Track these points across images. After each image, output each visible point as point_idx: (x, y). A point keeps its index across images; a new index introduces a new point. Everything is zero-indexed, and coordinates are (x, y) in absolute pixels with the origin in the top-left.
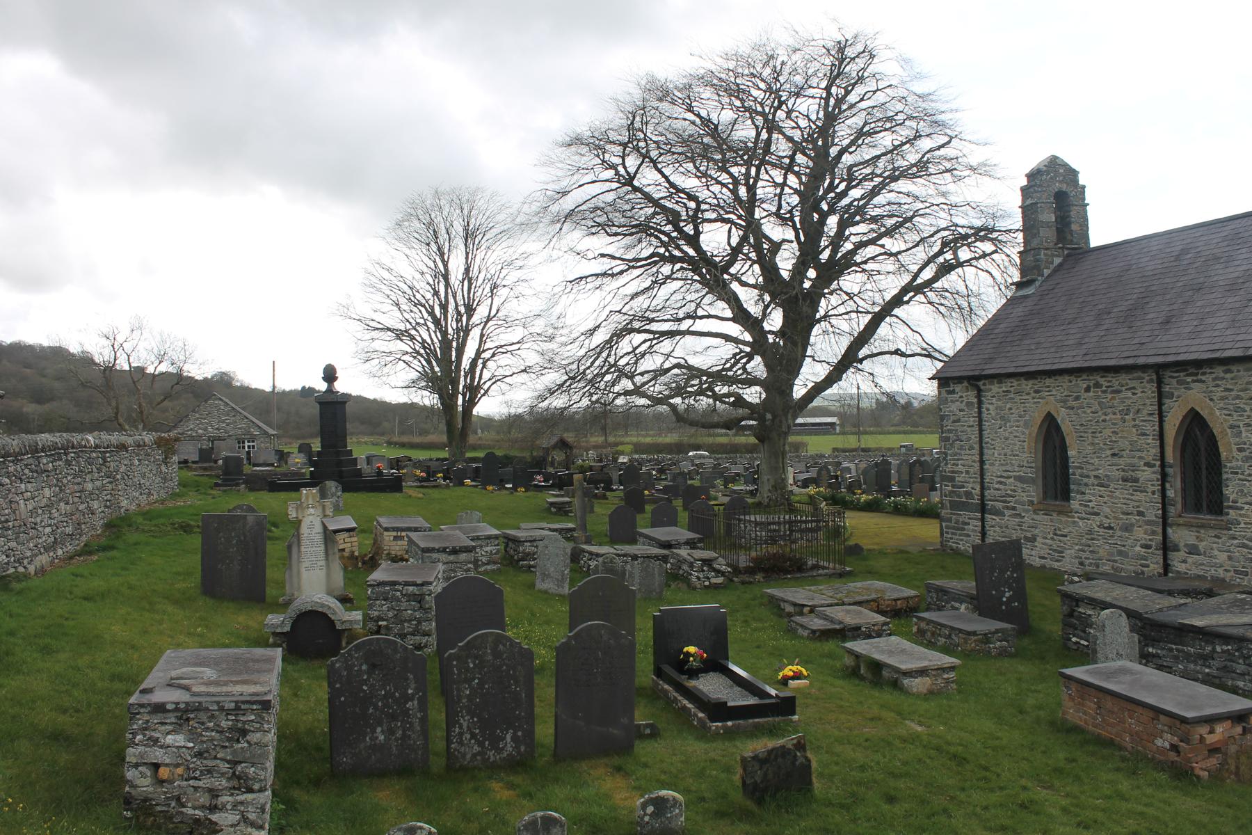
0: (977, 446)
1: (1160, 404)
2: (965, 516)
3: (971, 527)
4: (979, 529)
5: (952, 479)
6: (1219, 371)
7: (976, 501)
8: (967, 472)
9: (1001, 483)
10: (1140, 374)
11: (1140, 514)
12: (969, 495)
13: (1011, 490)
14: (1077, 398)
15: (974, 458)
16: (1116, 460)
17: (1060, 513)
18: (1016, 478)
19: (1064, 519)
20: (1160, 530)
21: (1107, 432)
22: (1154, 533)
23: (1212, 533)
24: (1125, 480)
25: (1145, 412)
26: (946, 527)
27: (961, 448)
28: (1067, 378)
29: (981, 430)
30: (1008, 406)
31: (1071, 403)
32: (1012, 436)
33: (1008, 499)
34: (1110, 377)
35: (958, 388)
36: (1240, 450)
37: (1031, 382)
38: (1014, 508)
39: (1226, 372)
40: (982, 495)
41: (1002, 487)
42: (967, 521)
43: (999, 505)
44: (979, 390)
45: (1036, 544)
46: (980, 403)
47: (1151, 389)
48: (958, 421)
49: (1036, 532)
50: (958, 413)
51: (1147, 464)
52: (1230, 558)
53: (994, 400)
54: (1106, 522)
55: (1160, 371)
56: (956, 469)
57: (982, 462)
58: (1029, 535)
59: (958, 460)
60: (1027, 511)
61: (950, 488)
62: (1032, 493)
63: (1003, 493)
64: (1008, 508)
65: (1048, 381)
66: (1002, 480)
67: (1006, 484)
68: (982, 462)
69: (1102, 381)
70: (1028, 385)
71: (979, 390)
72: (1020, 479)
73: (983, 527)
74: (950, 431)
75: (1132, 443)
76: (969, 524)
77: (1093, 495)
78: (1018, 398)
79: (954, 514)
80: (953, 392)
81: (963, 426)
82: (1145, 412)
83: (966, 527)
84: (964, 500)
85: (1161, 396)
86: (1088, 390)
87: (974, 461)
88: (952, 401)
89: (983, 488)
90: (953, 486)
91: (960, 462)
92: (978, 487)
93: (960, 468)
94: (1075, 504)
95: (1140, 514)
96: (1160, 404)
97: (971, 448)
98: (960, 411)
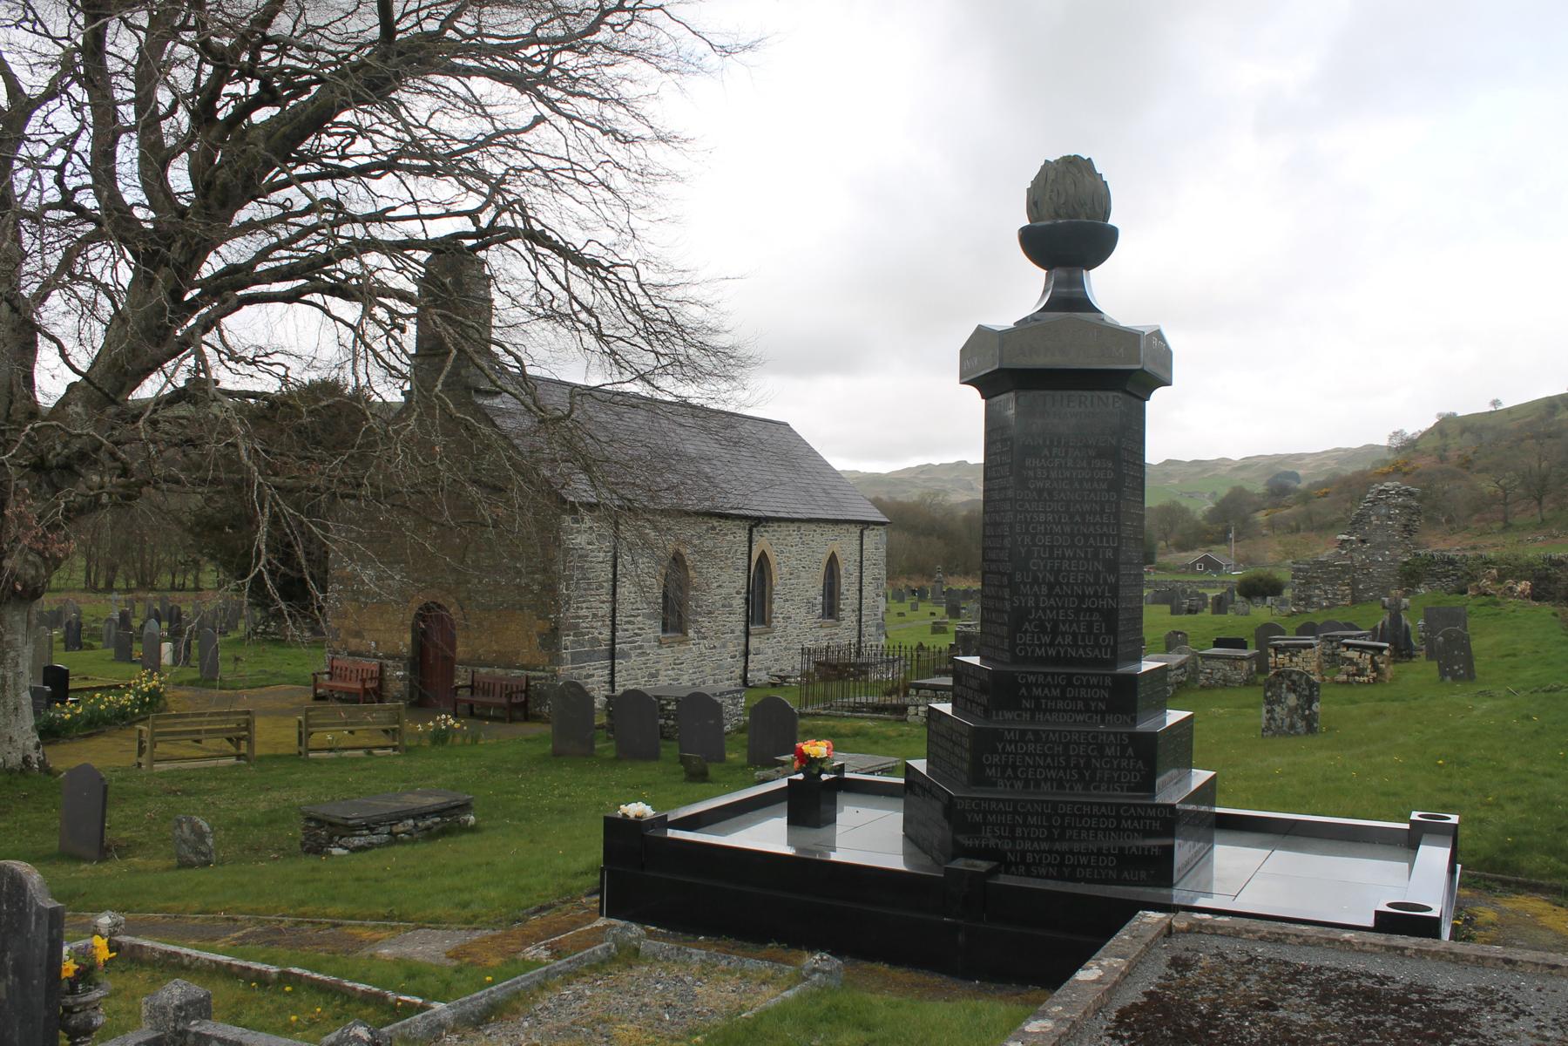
0: (608, 585)
3: (595, 678)
4: (607, 678)
10: (738, 522)
13: (639, 629)
17: (680, 643)
19: (683, 647)
20: (743, 641)
22: (739, 644)
23: (766, 636)
33: (636, 639)
36: (781, 578)
38: (641, 647)
39: (779, 527)
40: (613, 640)
41: (630, 627)
45: (660, 678)
47: (742, 535)
49: (658, 666)
51: (738, 593)
52: (773, 652)
55: (757, 522)
59: (584, 602)
61: (571, 638)
64: (635, 648)
66: (632, 619)
67: (634, 623)
73: (612, 674)
76: (593, 675)
79: (576, 668)
81: (591, 562)
83: (589, 680)
85: (750, 541)
87: (603, 602)
89: (613, 633)
91: (584, 605)
92: (607, 633)
93: (583, 612)
94: (691, 633)
98: (589, 544)
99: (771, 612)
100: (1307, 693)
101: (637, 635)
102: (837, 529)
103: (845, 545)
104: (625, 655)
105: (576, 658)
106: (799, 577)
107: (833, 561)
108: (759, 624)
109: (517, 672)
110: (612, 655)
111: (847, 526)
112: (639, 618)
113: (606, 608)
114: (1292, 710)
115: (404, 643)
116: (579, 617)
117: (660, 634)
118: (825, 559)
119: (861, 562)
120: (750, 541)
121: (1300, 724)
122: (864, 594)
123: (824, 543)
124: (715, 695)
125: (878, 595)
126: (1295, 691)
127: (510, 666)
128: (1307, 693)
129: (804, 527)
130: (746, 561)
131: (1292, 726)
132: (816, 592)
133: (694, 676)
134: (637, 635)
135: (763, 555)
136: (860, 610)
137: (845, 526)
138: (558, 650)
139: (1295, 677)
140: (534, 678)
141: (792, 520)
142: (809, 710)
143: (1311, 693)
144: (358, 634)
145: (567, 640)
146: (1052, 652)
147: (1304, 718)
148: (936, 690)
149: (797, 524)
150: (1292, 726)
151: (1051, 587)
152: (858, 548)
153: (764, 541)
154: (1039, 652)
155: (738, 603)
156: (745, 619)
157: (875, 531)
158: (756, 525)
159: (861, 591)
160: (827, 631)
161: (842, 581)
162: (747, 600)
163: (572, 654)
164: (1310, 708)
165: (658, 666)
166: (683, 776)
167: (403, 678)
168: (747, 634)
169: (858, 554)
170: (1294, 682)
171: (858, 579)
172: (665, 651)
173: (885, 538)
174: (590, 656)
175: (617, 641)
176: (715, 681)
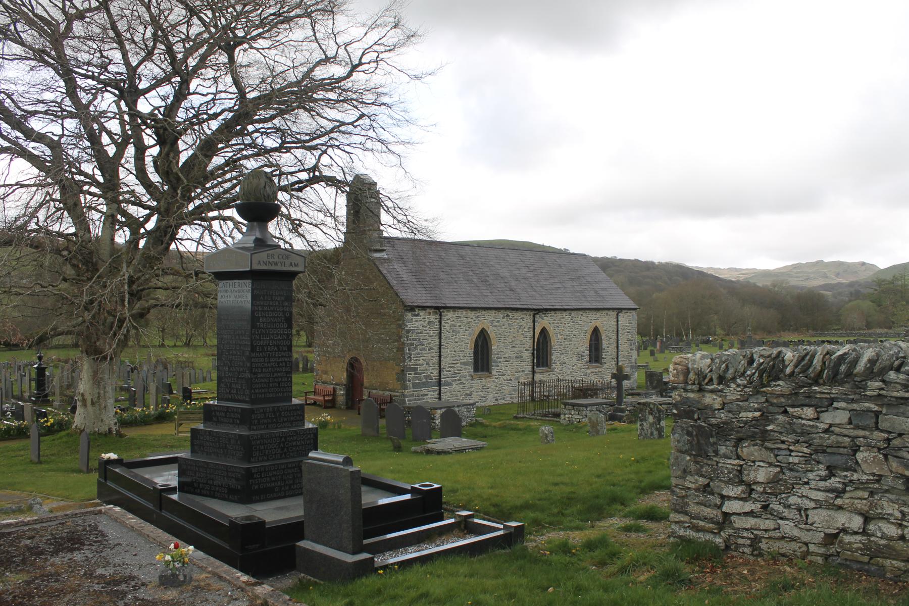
0: (436, 348)
1: (534, 325)
2: (424, 391)
3: (429, 396)
4: (437, 396)
5: (416, 369)
6: (553, 313)
7: (435, 380)
8: (427, 364)
9: (451, 367)
10: (525, 312)
11: (523, 371)
12: (427, 377)
14: (498, 321)
15: (432, 355)
16: (514, 349)
17: (486, 377)
18: (461, 363)
19: (488, 380)
20: (531, 376)
21: (511, 337)
22: (528, 378)
24: (516, 357)
25: (527, 328)
26: (409, 401)
27: (424, 349)
28: (494, 311)
29: (440, 338)
30: (458, 324)
31: (495, 323)
32: (460, 341)
34: (514, 312)
35: (422, 313)
37: (473, 313)
38: (459, 380)
40: (440, 376)
42: (426, 393)
43: (449, 380)
44: (441, 315)
46: (440, 322)
47: (530, 319)
48: (421, 333)
49: (472, 390)
50: (421, 328)
51: (526, 350)
53: (449, 321)
54: (509, 378)
55: (537, 311)
56: (418, 362)
57: (440, 356)
58: (468, 392)
60: (467, 380)
62: (471, 369)
63: (452, 372)
64: (456, 380)
65: (483, 312)
68: (440, 356)
69: (510, 314)
70: (472, 314)
71: (441, 315)
72: (464, 364)
73: (440, 394)
74: (414, 339)
75: (521, 342)
77: (503, 367)
78: (465, 320)
80: (418, 315)
82: (527, 328)
84: (424, 380)
85: (534, 321)
86: (503, 318)
88: (416, 321)
89: (440, 372)
90: (415, 374)
92: (436, 373)
93: (421, 362)
94: (494, 372)
95: (523, 371)
96: (534, 325)
97: (431, 349)
99: (551, 360)
100: (657, 415)
101: (456, 373)
102: (599, 314)
103: (606, 323)
104: (448, 384)
105: (416, 386)
106: (571, 341)
107: (596, 332)
108: (543, 366)
109: (387, 393)
110: (439, 384)
111: (607, 311)
112: (459, 365)
113: (436, 360)
114: (652, 425)
115: (343, 377)
116: (417, 365)
117: (473, 373)
118: (590, 330)
119: (617, 331)
120: (534, 321)
121: (656, 433)
122: (620, 349)
123: (589, 322)
124: (454, 406)
125: (631, 349)
126: (652, 414)
127: (385, 390)
128: (657, 415)
129: (573, 313)
130: (532, 333)
131: (652, 434)
132: (584, 349)
133: (497, 395)
134: (456, 373)
135: (544, 332)
136: (617, 358)
137: (604, 312)
138: (405, 381)
139: (652, 406)
140: (394, 396)
141: (565, 310)
142: (521, 416)
143: (660, 415)
144: (326, 373)
145: (410, 376)
146: (230, 396)
147: (657, 429)
148: (574, 406)
149: (568, 312)
150: (652, 434)
151: (229, 368)
152: (615, 323)
153: (544, 321)
154: (226, 396)
155: (527, 355)
156: (531, 364)
157: (628, 314)
158: (537, 314)
159: (617, 347)
160: (593, 370)
161: (604, 342)
162: (533, 354)
163: (413, 384)
164: (659, 424)
165: (472, 390)
166: (392, 448)
167: (343, 395)
168: (534, 372)
169: (615, 327)
170: (651, 409)
171: (615, 341)
172: (477, 382)
173: (636, 317)
174: (425, 385)
175: (442, 376)
176: (511, 398)
